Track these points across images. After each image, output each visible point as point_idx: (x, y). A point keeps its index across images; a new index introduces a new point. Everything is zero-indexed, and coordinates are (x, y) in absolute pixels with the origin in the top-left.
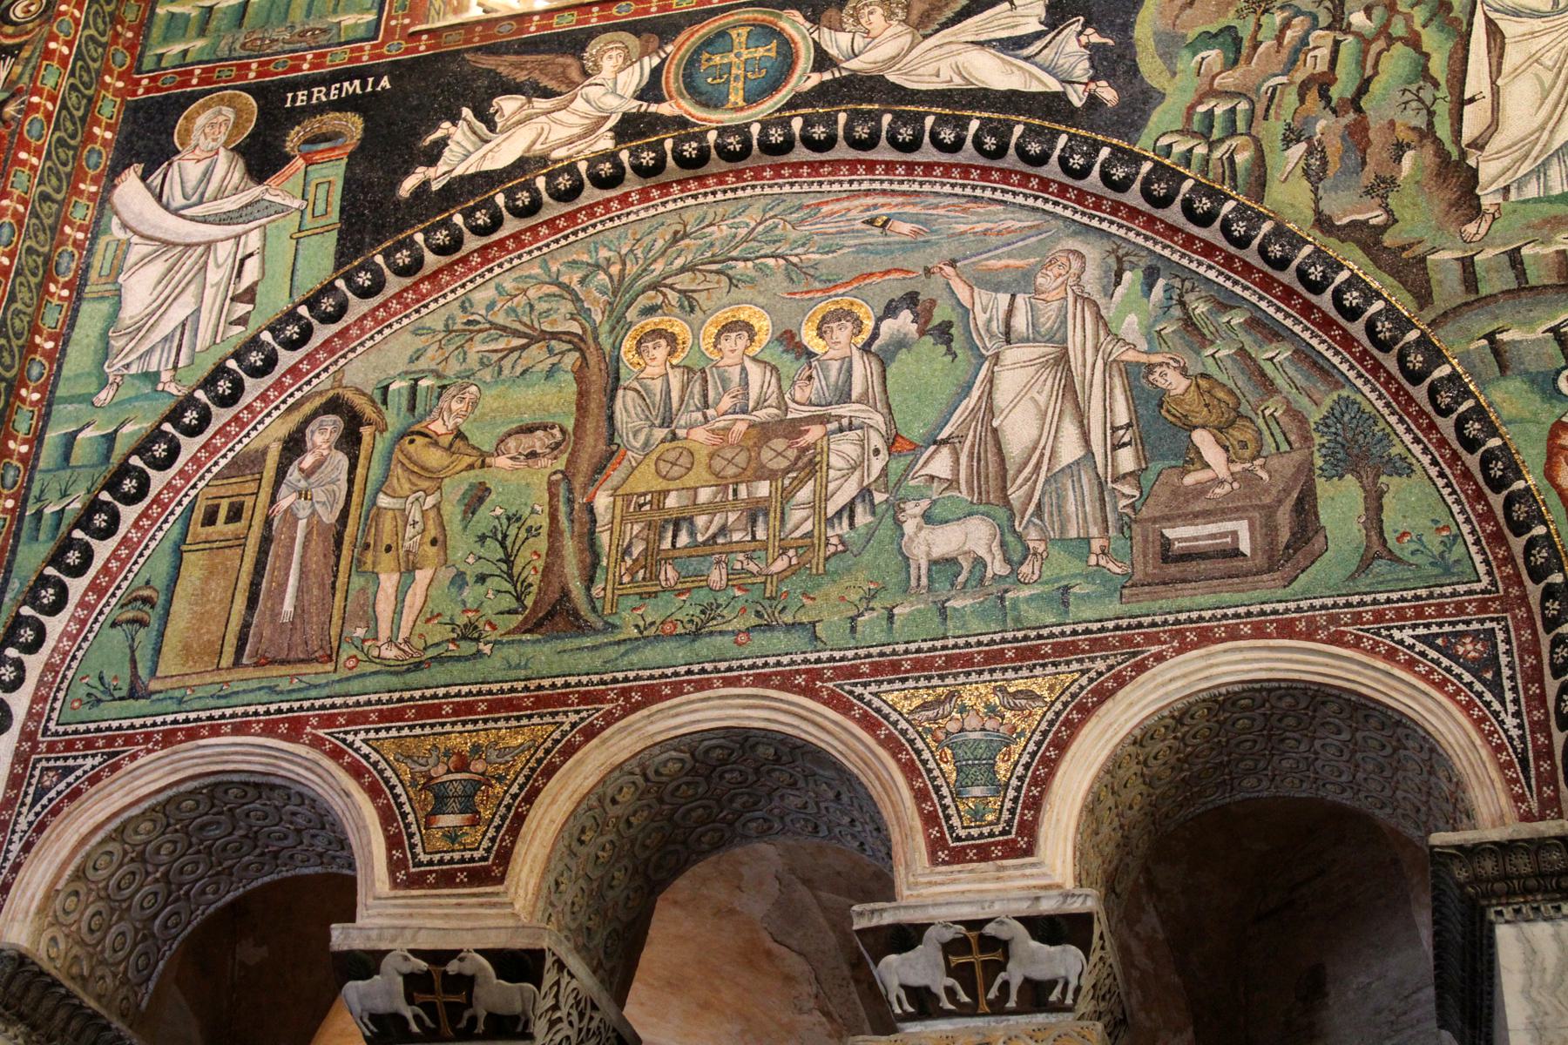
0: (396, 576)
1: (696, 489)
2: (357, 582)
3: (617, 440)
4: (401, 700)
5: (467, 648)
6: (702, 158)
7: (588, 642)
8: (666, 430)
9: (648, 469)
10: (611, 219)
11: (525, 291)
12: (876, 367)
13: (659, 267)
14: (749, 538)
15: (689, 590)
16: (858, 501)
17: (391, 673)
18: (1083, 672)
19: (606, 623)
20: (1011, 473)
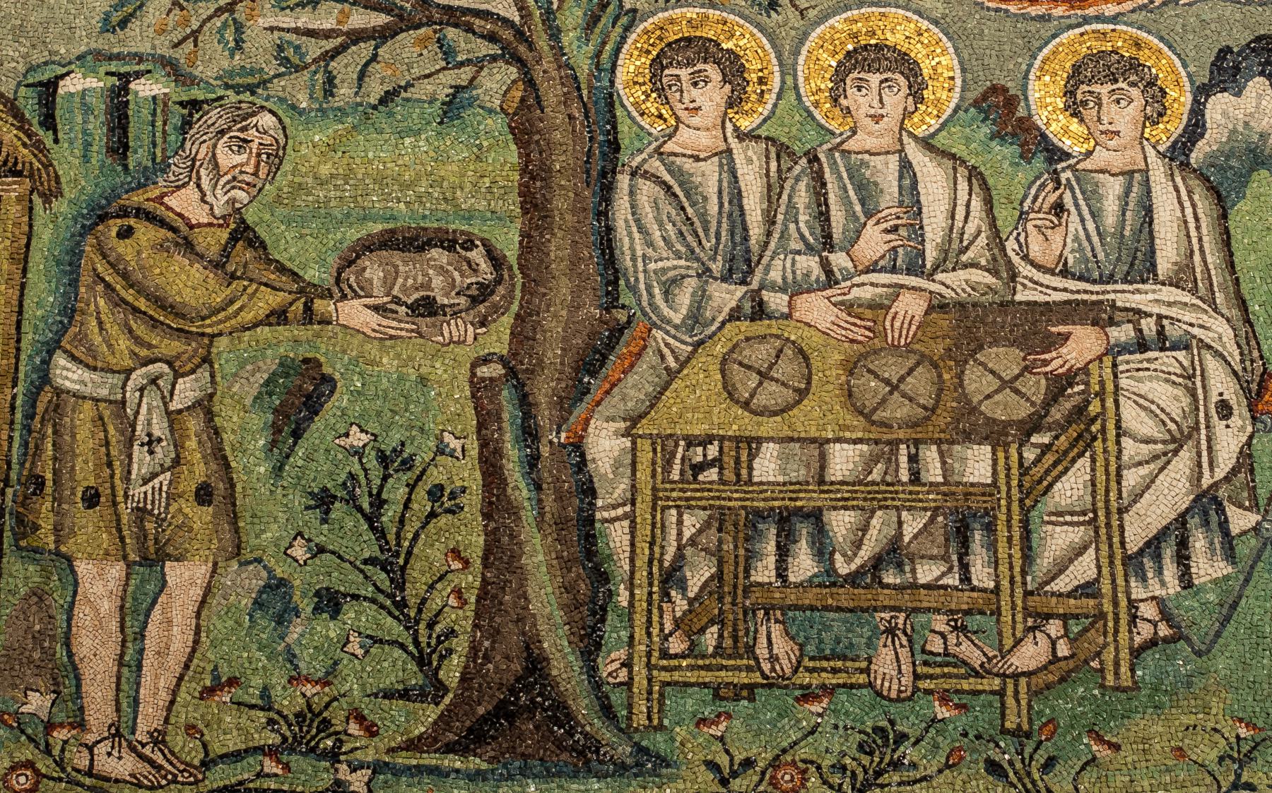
1: (822, 443)
3: (626, 298)
12: (1204, 205)
14: (953, 580)
15: (829, 690)
16: (1193, 522)
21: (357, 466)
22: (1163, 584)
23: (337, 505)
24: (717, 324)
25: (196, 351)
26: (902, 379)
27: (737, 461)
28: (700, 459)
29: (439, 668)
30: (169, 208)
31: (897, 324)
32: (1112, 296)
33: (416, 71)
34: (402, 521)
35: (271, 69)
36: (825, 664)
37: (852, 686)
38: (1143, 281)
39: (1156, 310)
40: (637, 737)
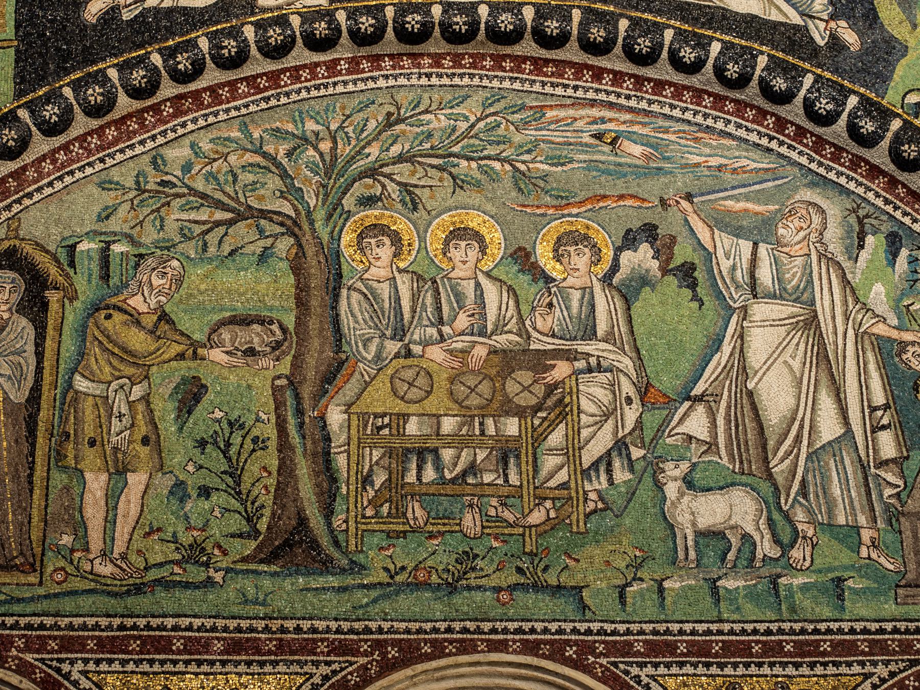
0: (104, 477)
1: (438, 416)
2: (59, 479)
3: (345, 348)
4: (122, 627)
5: (196, 574)
6: (424, 34)
7: (333, 581)
8: (400, 344)
9: (382, 386)
10: (317, 88)
11: (225, 156)
13: (374, 151)
14: (500, 481)
15: (441, 534)
16: (614, 453)
17: (109, 594)
18: (867, 676)
19: (352, 562)
20: (771, 443)
21: (218, 427)
22: (600, 483)
23: (209, 446)
24: (388, 360)
25: (141, 373)
26: (476, 386)
27: (398, 425)
28: (380, 424)
29: (257, 523)
30: (129, 305)
31: (474, 360)
32: (575, 347)
33: (246, 240)
34: (239, 453)
35: (177, 239)
36: (440, 521)
37: (452, 532)
38: (591, 340)
39: (596, 353)
40: (350, 556)
